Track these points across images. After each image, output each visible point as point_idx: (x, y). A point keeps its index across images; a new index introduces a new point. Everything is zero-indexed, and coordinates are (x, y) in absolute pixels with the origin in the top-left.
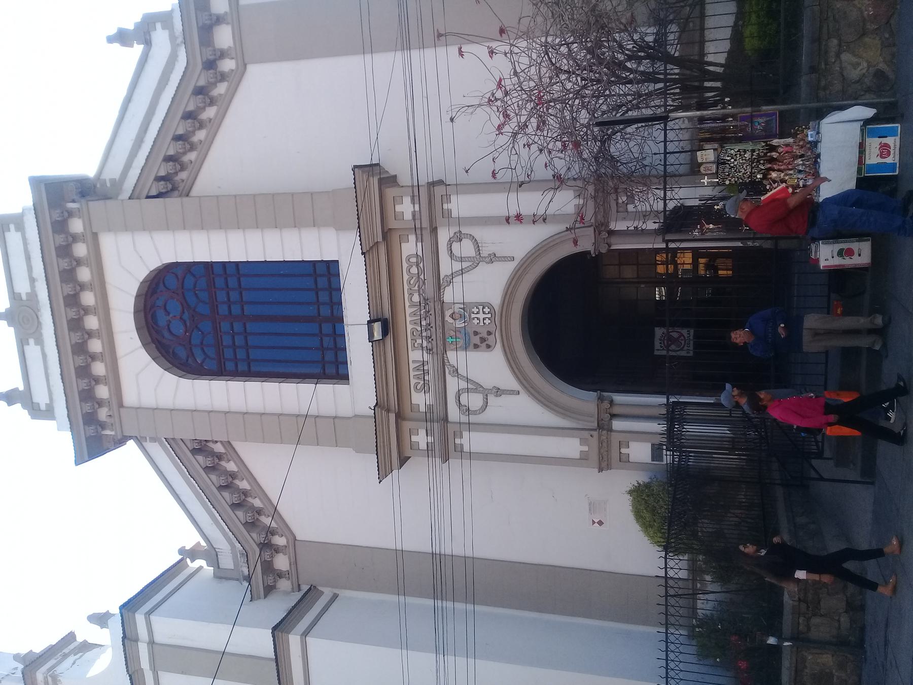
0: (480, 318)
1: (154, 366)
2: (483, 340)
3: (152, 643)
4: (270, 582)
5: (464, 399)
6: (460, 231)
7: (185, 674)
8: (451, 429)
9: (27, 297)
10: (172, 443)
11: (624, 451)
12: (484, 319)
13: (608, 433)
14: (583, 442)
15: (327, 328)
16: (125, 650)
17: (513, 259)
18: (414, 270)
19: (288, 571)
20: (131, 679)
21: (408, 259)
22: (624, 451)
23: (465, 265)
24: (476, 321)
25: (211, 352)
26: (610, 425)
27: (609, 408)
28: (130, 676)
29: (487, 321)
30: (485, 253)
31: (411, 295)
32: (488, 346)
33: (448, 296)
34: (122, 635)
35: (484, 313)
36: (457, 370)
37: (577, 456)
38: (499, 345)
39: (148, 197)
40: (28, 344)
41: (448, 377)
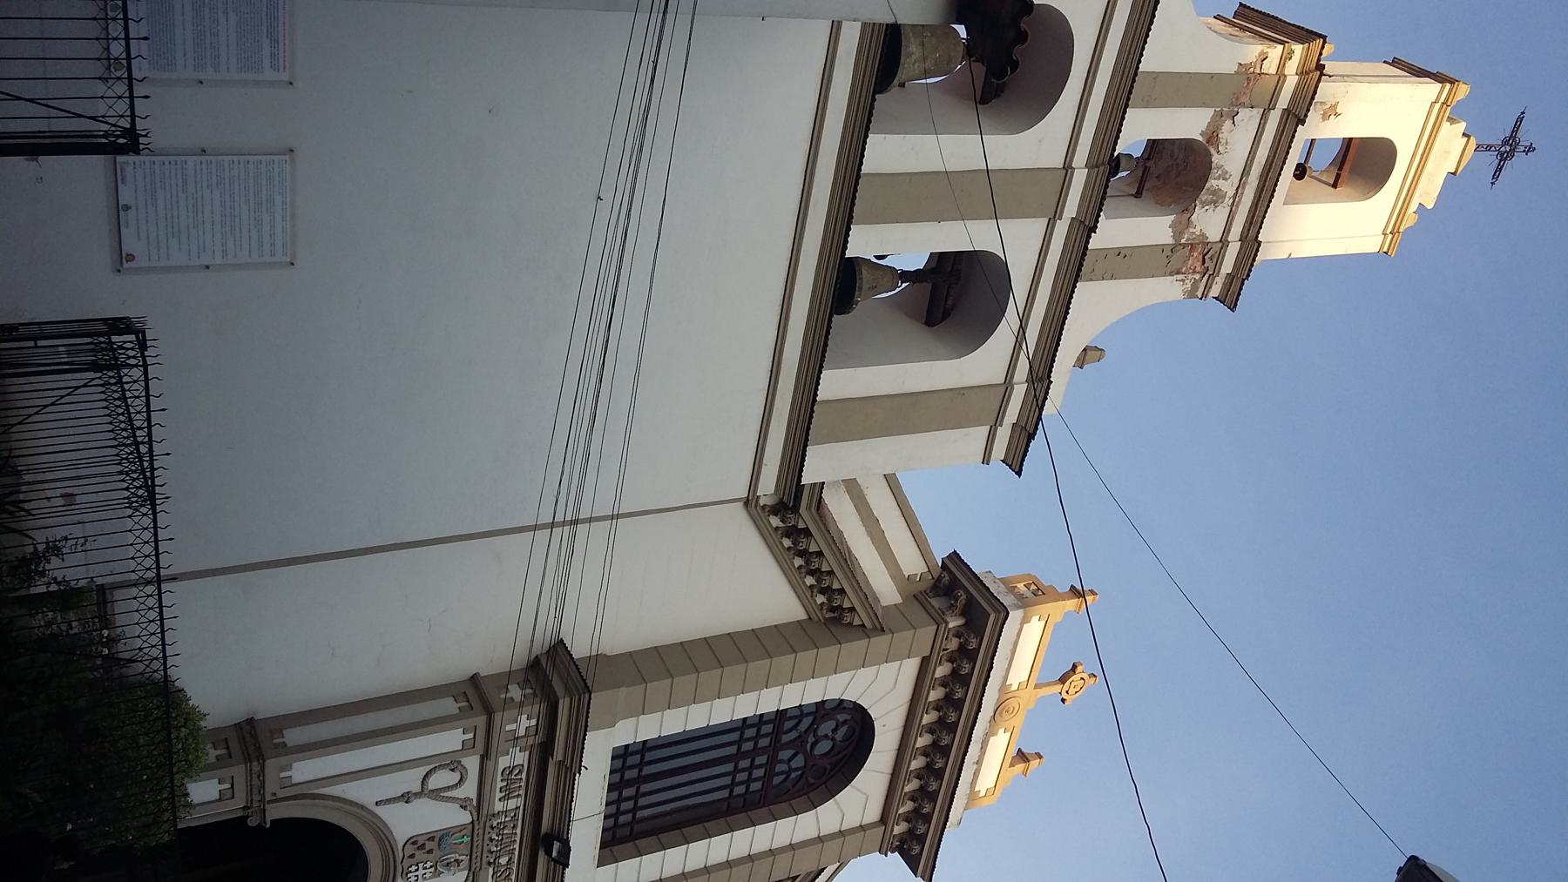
5: (456, 777)
12: (417, 870)
13: (252, 803)
14: (287, 784)
20: (1050, 371)
27: (248, 817)
28: (1049, 377)
32: (414, 843)
36: (461, 807)
37: (295, 765)
41: (473, 795)
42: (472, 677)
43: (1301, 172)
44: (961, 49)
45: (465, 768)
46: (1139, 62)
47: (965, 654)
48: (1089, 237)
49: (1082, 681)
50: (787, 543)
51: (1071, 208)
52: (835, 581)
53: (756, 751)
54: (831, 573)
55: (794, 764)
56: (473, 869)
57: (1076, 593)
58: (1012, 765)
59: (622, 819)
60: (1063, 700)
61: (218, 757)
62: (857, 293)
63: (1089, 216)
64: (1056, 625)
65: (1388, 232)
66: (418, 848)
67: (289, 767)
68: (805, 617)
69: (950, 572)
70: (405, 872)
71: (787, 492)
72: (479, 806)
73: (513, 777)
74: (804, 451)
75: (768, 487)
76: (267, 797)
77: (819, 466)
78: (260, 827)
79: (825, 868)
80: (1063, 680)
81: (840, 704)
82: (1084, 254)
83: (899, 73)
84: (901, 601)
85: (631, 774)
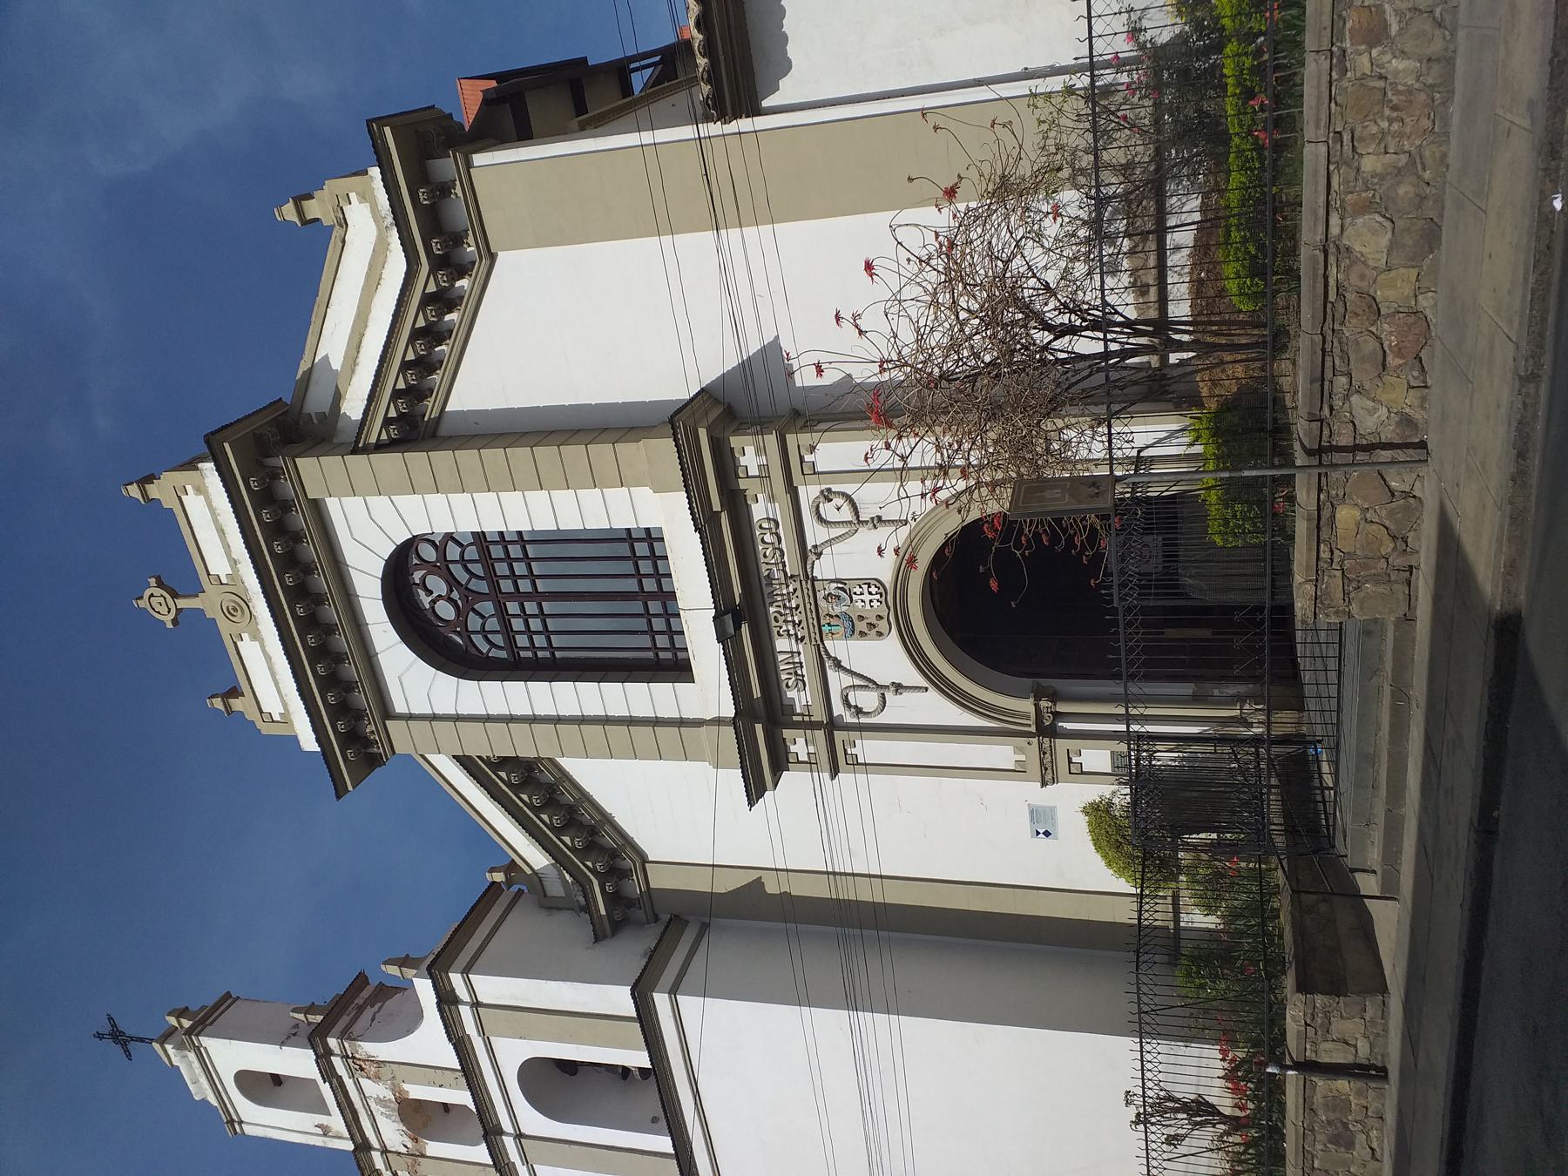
0: (866, 603)
2: (872, 626)
3: (476, 1005)
4: (617, 916)
6: (829, 490)
7: (525, 1039)
8: (839, 736)
9: (227, 579)
10: (465, 762)
12: (871, 601)
14: (1018, 750)
15: (655, 607)
16: (442, 1017)
18: (768, 538)
19: (638, 899)
20: (455, 1048)
23: (836, 532)
24: (860, 604)
25: (498, 639)
26: (1053, 725)
29: (875, 604)
32: (880, 634)
34: (436, 1000)
35: (870, 593)
36: (840, 662)
38: (894, 631)
39: (379, 447)
48: (485, 1129)
53: (518, 595)
54: (537, 810)
56: (809, 582)
60: (160, 584)
65: (202, 1049)
66: (875, 626)
70: (883, 599)
72: (823, 660)
73: (794, 679)
80: (179, 611)
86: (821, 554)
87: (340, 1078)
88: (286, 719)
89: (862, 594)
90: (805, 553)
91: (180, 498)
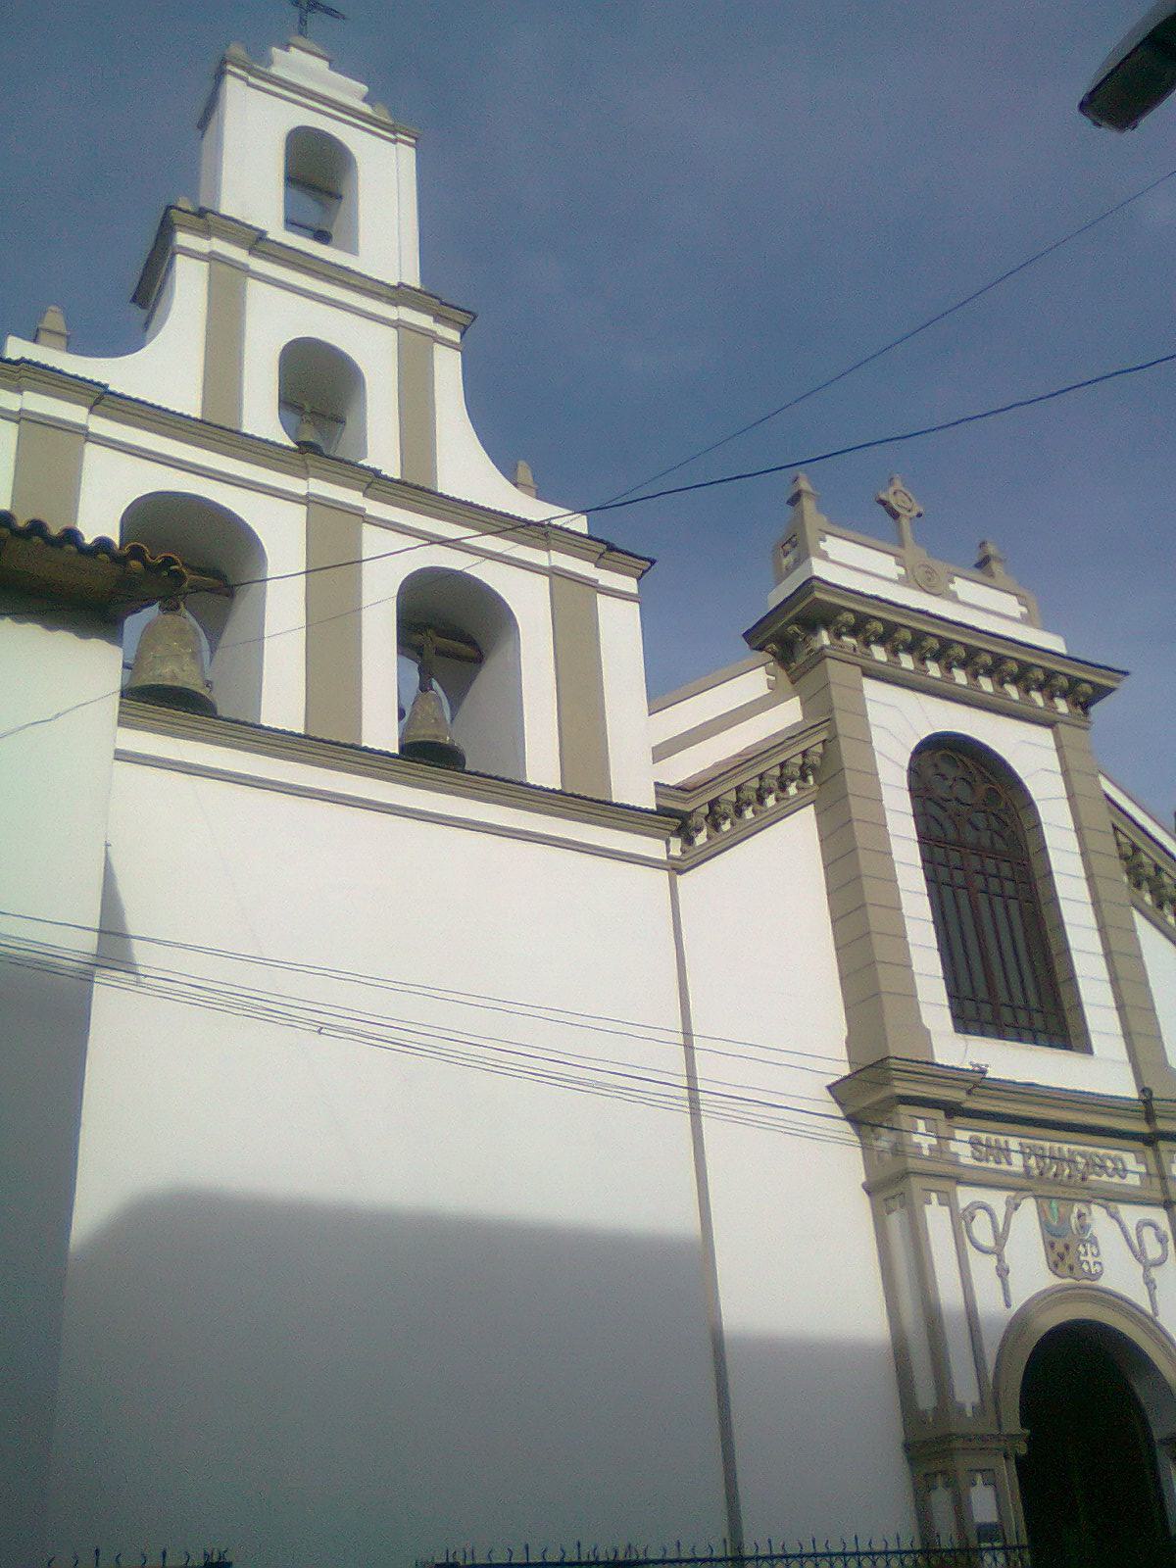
1: (917, 742)
2: (1062, 1257)
5: (981, 1215)
11: (979, 1479)
12: (1088, 1263)
14: (980, 1409)
17: (1156, 1314)
18: (1109, 1164)
21: (1121, 1160)
22: (979, 1479)
30: (1154, 1273)
31: (1083, 1155)
32: (1056, 1265)
33: (1094, 1207)
35: (1095, 1263)
36: (1016, 1209)
38: (1058, 1281)
40: (897, 564)
42: (869, 1193)
43: (323, 237)
44: (169, 617)
45: (972, 1204)
46: (188, 417)
47: (859, 627)
48: (386, 478)
49: (898, 494)
50: (726, 826)
51: (353, 497)
52: (770, 772)
55: (982, 825)
57: (795, 499)
58: (992, 575)
59: (1039, 1023)
60: (919, 515)
61: (947, 1485)
62: (441, 741)
63: (361, 477)
64: (831, 521)
67: (961, 1409)
68: (812, 807)
69: (768, 641)
71: (662, 826)
72: (1018, 1187)
74: (616, 805)
75: (653, 847)
76: (996, 1432)
77: (633, 785)
78: (1030, 1442)
79: (1107, 797)
80: (895, 515)
81: (914, 771)
82: (405, 484)
83: (194, 688)
84: (797, 698)
85: (986, 1009)
86: (1113, 1217)
87: (394, 303)
88: (824, 556)
89: (1093, 1254)
90: (1111, 1198)
91: (1016, 595)
